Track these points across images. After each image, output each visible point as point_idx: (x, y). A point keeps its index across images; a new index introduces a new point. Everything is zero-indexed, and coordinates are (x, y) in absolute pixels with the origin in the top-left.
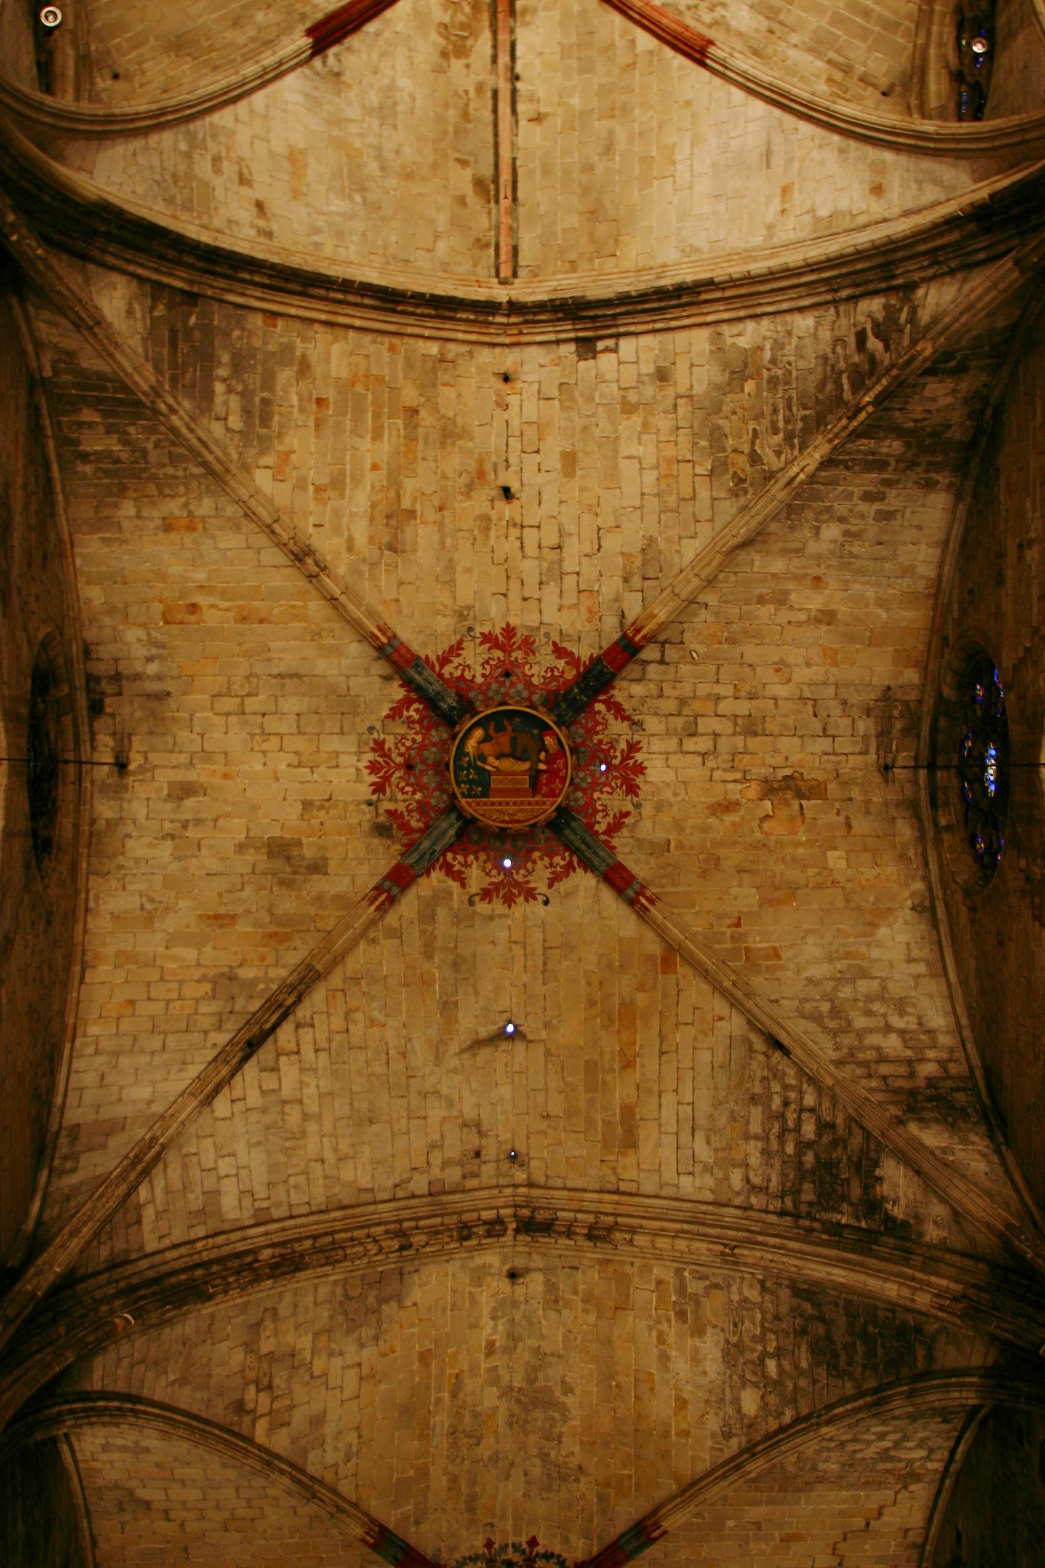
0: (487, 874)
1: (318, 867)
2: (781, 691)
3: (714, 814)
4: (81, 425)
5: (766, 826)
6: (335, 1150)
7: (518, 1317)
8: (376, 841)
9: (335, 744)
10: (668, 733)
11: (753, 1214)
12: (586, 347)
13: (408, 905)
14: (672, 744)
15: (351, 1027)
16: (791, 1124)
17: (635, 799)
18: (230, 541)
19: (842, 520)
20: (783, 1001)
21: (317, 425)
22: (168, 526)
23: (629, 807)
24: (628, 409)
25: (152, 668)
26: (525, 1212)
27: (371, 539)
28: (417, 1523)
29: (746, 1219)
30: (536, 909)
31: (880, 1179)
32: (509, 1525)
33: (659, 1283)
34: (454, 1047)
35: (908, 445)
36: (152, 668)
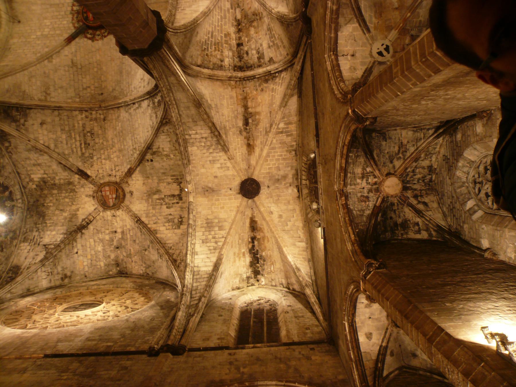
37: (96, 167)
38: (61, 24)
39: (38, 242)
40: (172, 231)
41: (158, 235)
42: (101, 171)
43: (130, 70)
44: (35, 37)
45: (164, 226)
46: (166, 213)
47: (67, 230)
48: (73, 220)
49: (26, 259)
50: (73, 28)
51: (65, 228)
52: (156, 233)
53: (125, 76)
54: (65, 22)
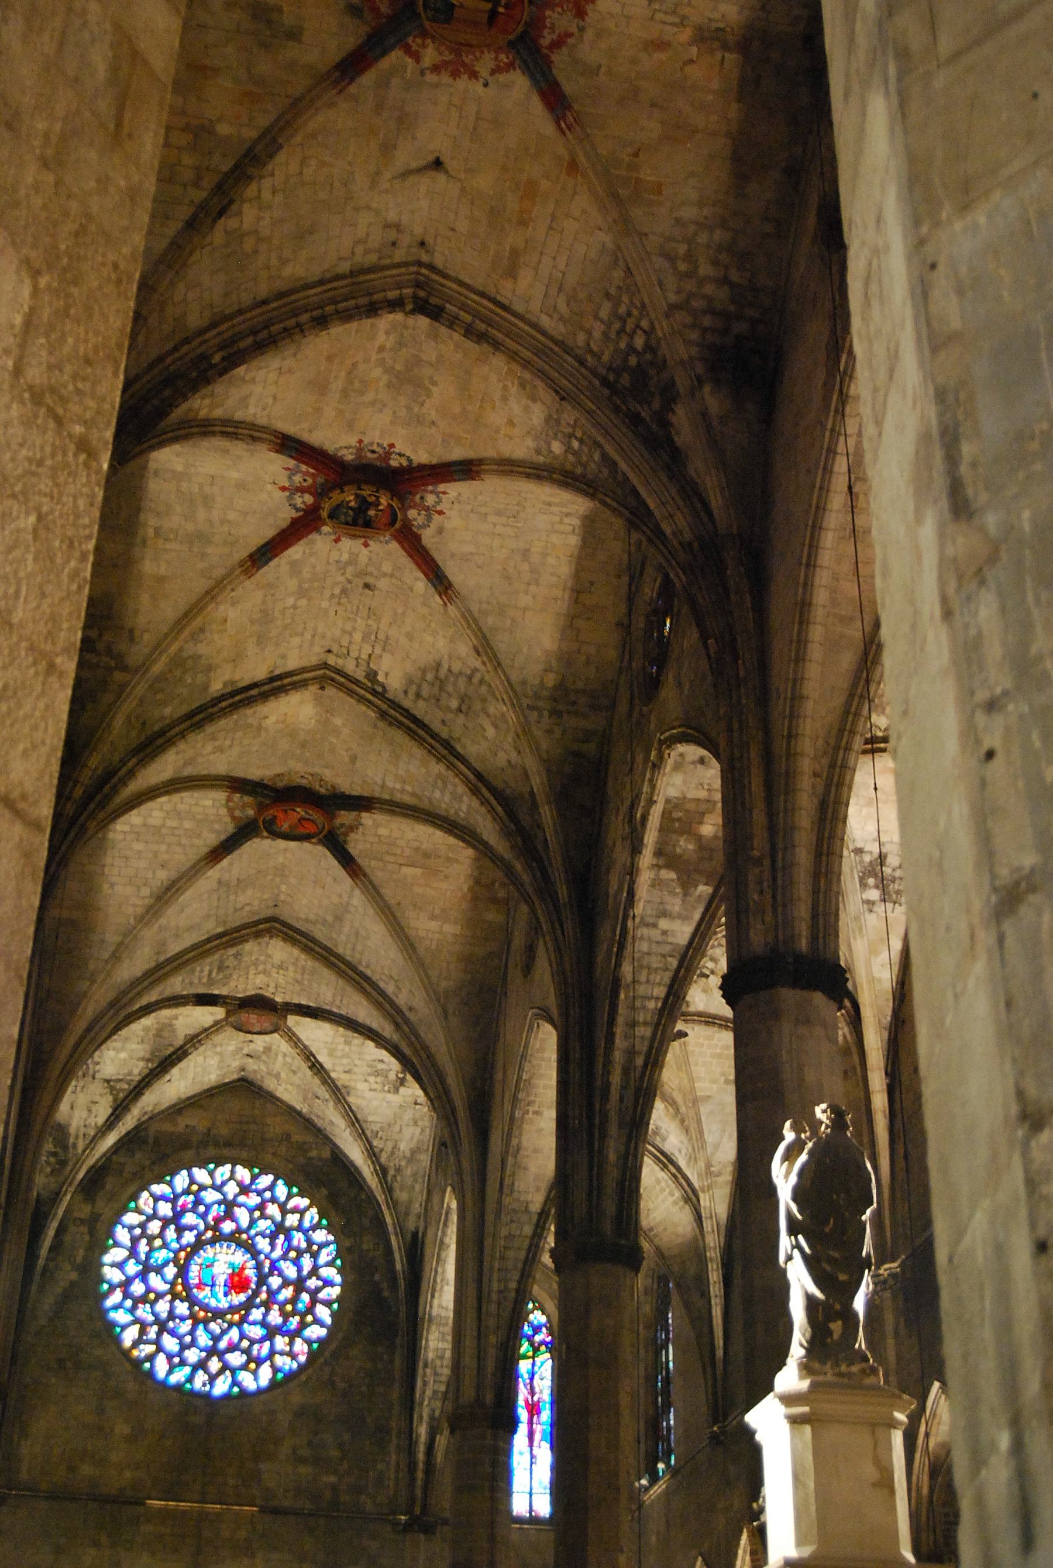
0: (440, 54)
1: (294, 35)
3: (645, 49)
5: (688, 69)
6: (280, 258)
7: (406, 334)
8: (347, 19)
11: (583, 370)
13: (367, 79)
15: (304, 171)
16: (628, 329)
17: (581, 23)
20: (651, 236)
23: (574, 29)
26: (422, 294)
28: (310, 431)
29: (578, 371)
30: (477, 87)
31: (673, 411)
32: (378, 433)
34: (388, 175)
37: (232, 984)
38: (197, 804)
39: (91, 1072)
40: (381, 1095)
41: (350, 1099)
42: (241, 987)
43: (363, 933)
44: (127, 828)
45: (366, 1081)
46: (373, 1057)
47: (152, 1053)
48: (165, 1034)
49: (72, 1108)
50: (228, 819)
51: (147, 1047)
52: (348, 1094)
53: (346, 929)
54: (209, 803)
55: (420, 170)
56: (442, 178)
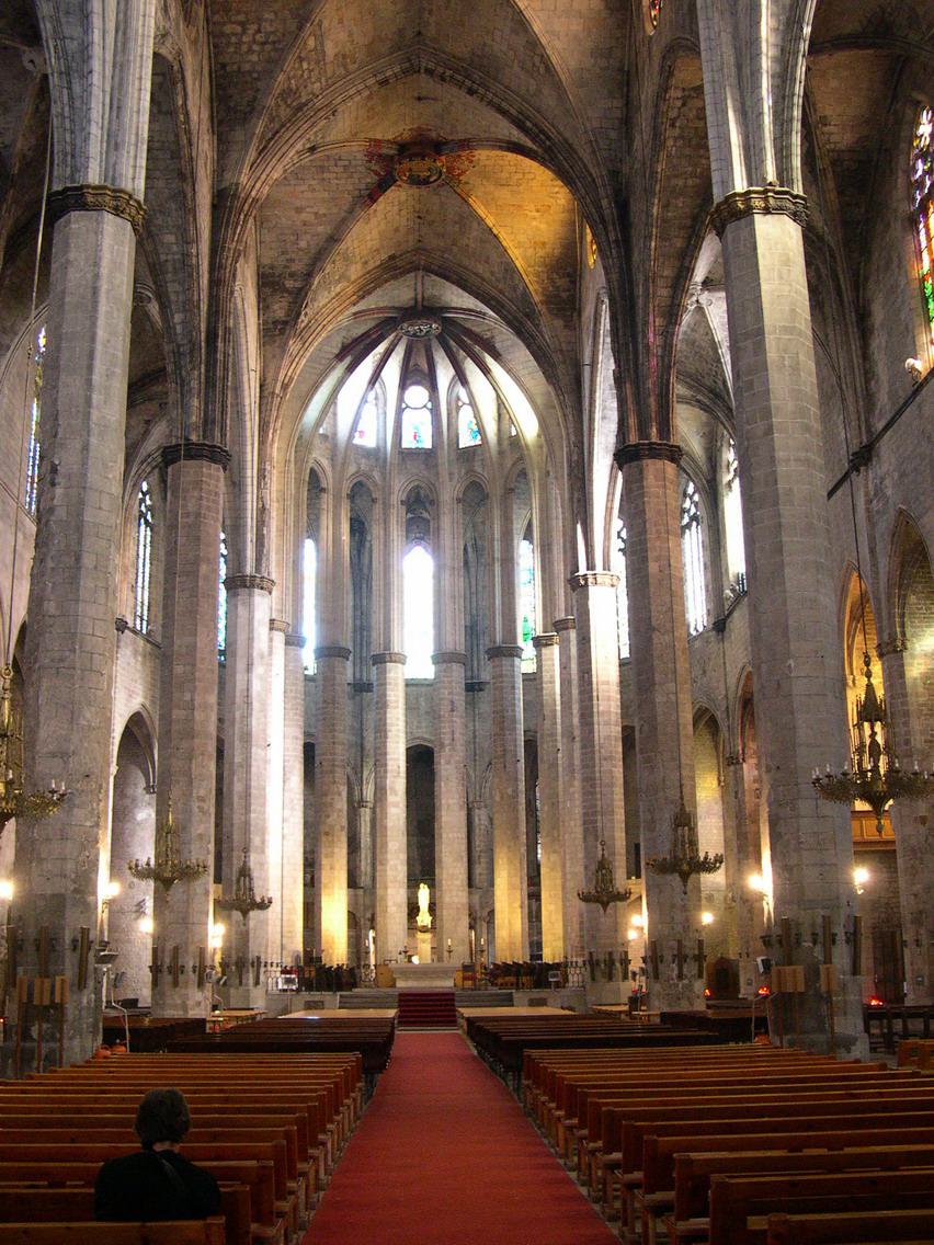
2: (313, 182)
4: (569, 290)
9: (487, 163)
10: (356, 166)
12: (392, 258)
14: (354, 162)
18: (522, 238)
19: (300, 249)
21: (488, 258)
22: (544, 244)
24: (377, 250)
25: (556, 189)
27: (471, 222)
33: (355, 63)
35: (283, 284)
36: (556, 189)
55: (426, 98)
56: (416, 95)
